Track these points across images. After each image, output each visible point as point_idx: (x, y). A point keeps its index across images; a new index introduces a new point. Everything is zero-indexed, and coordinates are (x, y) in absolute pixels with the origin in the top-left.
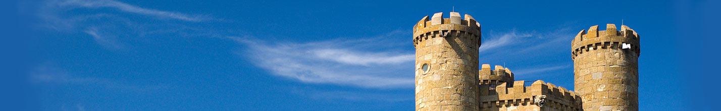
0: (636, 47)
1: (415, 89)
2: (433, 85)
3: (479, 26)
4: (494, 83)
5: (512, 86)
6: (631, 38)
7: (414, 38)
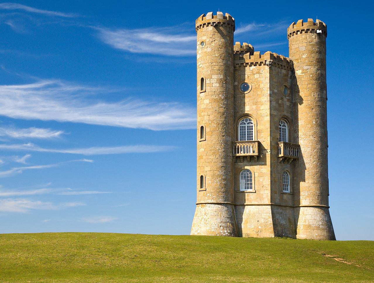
0: (325, 32)
1: (197, 56)
2: (207, 54)
3: (234, 20)
4: (242, 53)
5: (253, 55)
6: (322, 27)
7: (196, 26)
